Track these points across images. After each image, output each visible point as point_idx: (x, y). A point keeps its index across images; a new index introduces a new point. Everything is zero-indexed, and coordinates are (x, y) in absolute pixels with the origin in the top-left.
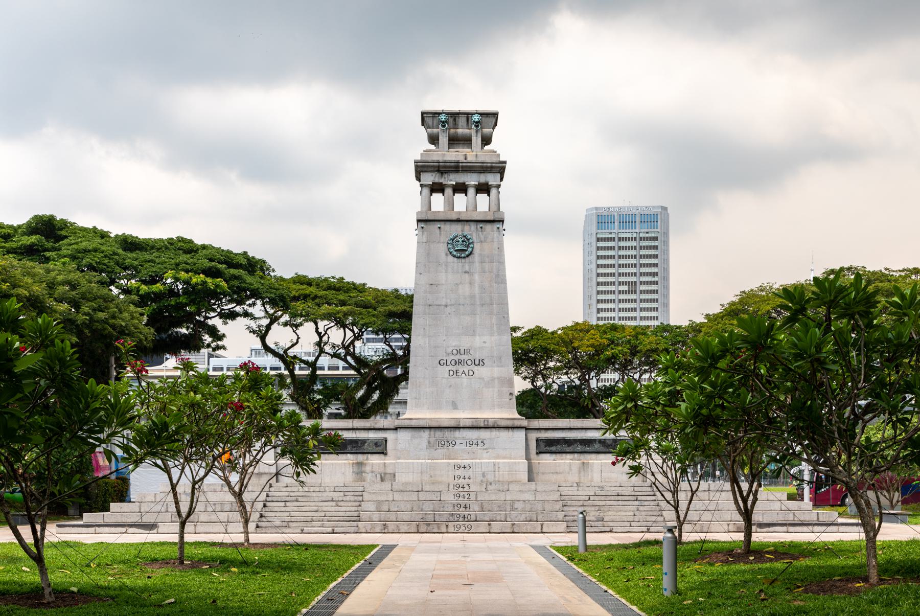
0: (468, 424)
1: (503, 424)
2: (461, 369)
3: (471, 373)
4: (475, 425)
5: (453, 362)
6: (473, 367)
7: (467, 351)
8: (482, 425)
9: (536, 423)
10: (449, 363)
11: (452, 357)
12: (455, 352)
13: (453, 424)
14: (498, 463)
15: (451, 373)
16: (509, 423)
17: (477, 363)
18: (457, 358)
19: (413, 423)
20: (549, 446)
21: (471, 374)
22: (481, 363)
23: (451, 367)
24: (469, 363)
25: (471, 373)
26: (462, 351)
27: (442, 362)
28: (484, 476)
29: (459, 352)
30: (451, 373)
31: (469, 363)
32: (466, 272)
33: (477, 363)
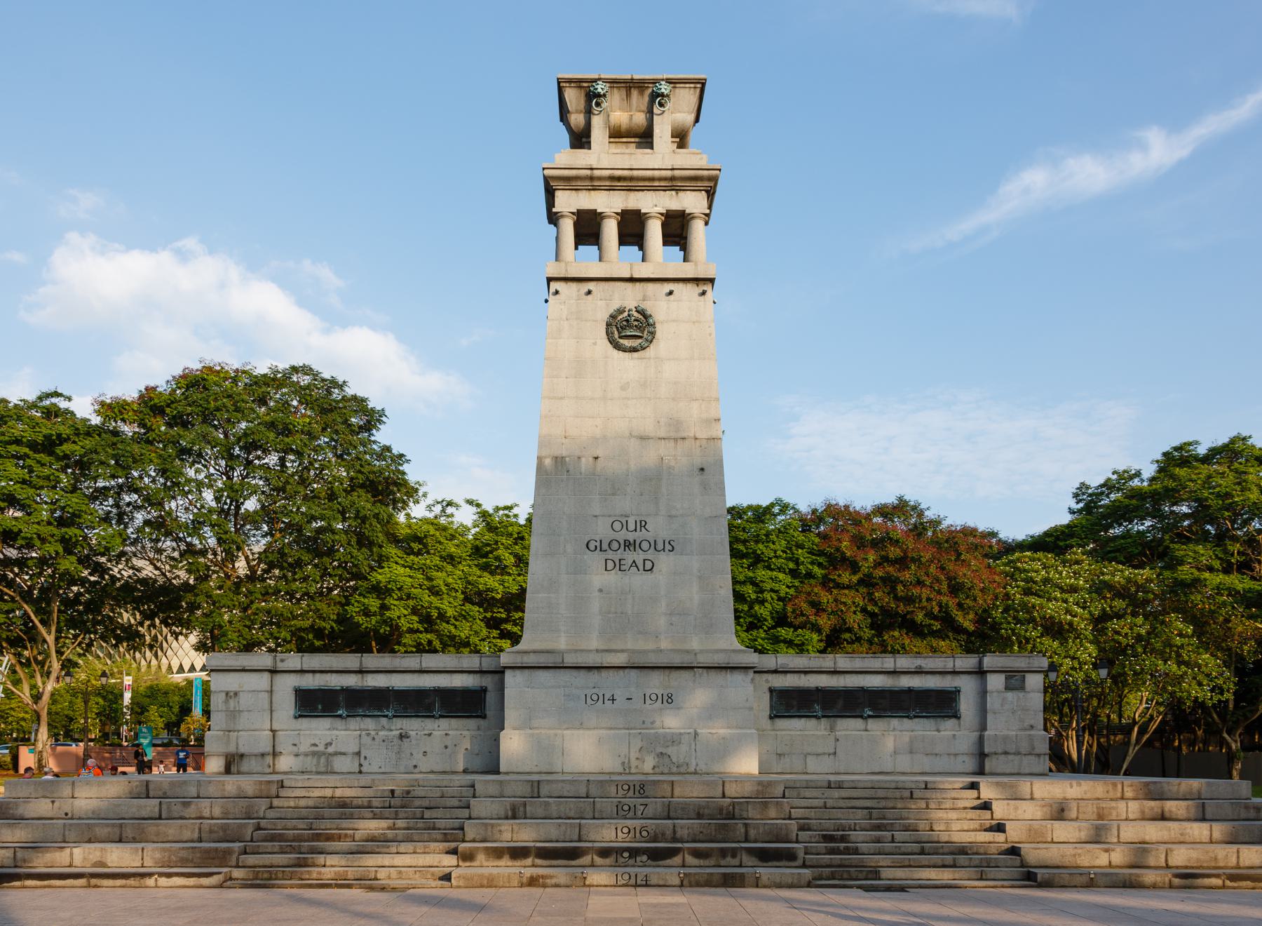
2: (630, 556)
6: (651, 555)
9: (769, 661)
10: (605, 546)
15: (610, 565)
16: (719, 659)
18: (623, 535)
20: (789, 703)
23: (610, 555)
26: (632, 527)
27: (592, 547)
30: (610, 565)
31: (645, 545)
33: (660, 547)
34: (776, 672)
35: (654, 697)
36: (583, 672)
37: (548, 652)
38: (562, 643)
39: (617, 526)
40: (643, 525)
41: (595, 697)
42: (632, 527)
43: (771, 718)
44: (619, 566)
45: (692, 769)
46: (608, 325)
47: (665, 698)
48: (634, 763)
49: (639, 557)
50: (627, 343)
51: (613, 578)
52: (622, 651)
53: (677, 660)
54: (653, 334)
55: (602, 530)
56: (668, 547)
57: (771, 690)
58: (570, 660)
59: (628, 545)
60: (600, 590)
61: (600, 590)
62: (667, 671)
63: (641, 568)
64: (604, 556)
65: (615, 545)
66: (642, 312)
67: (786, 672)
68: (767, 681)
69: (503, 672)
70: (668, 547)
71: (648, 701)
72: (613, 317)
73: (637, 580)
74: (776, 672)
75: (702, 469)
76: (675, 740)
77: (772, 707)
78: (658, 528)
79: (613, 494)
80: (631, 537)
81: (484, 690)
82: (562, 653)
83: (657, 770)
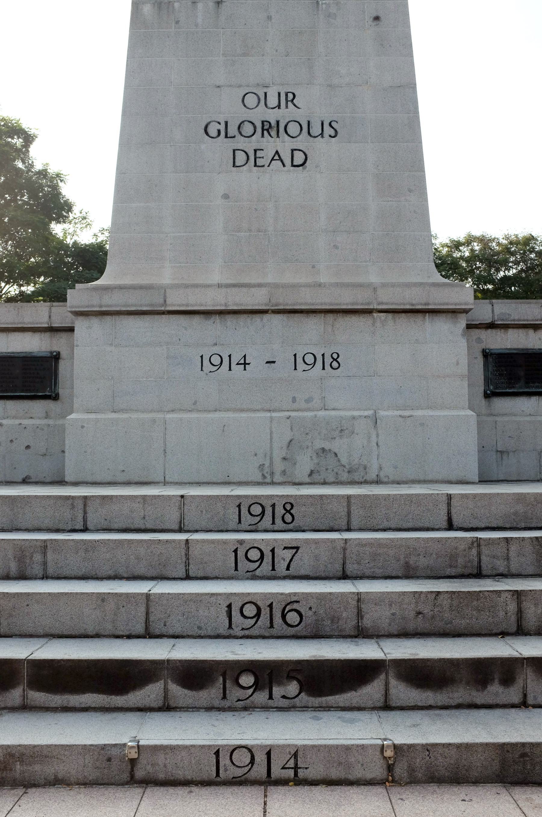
2: (270, 145)
10: (233, 130)
15: (241, 158)
16: (415, 298)
18: (259, 114)
23: (241, 143)
25: (299, 158)
26: (273, 101)
27: (213, 131)
30: (241, 158)
31: (293, 129)
33: (316, 130)
34: (492, 326)
35: (310, 359)
36: (196, 320)
37: (141, 287)
38: (166, 277)
39: (251, 100)
40: (291, 98)
41: (216, 360)
42: (273, 101)
43: (487, 396)
44: (254, 158)
45: (372, 476)
47: (328, 360)
48: (279, 466)
49: (284, 145)
51: (247, 176)
52: (260, 285)
53: (346, 300)
55: (227, 108)
56: (328, 131)
57: (486, 354)
58: (176, 301)
59: (267, 128)
60: (226, 197)
61: (226, 197)
62: (330, 317)
64: (231, 144)
65: (248, 129)
67: (506, 327)
68: (479, 340)
70: (328, 131)
71: (301, 365)
73: (282, 179)
74: (492, 326)
75: (377, 18)
76: (343, 430)
77: (487, 381)
78: (312, 105)
79: (245, 55)
80: (272, 116)
81: (56, 357)
82: (163, 289)
83: (316, 477)
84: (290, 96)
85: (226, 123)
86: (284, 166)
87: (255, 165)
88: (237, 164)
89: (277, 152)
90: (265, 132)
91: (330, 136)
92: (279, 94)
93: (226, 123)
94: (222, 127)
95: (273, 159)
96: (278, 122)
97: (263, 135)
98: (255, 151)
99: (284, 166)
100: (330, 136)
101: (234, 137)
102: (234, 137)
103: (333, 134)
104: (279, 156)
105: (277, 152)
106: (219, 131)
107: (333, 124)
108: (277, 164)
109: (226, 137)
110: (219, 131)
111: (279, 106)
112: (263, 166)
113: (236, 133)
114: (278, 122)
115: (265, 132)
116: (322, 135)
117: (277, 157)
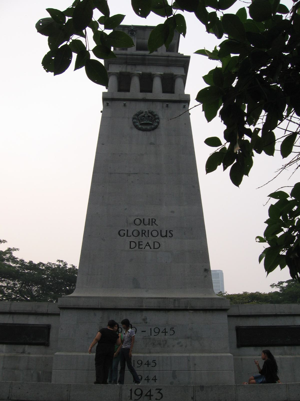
0: (153, 305)
1: (199, 305)
3: (157, 245)
4: (162, 306)
5: (135, 233)
7: (152, 222)
8: (171, 307)
10: (130, 233)
11: (134, 227)
12: (138, 222)
13: (132, 305)
14: (194, 358)
15: (133, 245)
17: (164, 234)
19: (81, 304)
21: (156, 247)
22: (169, 234)
23: (132, 239)
24: (155, 233)
25: (157, 245)
26: (147, 221)
27: (122, 233)
28: (174, 376)
29: (142, 221)
30: (133, 245)
32: (151, 144)
33: (164, 234)
46: (134, 118)
50: (144, 127)
54: (158, 123)
57: (238, 329)
59: (143, 233)
63: (152, 247)
66: (151, 113)
69: (59, 315)
70: (169, 234)
72: (137, 115)
84: (154, 220)
85: (127, 230)
86: (151, 248)
87: (139, 248)
88: (132, 247)
89: (148, 243)
90: (143, 235)
91: (169, 236)
92: (149, 219)
93: (127, 230)
94: (126, 232)
95: (146, 246)
96: (148, 231)
97: (142, 236)
98: (139, 242)
99: (151, 248)
100: (169, 236)
101: (130, 236)
102: (130, 236)
103: (171, 236)
104: (149, 244)
105: (148, 243)
106: (124, 234)
107: (171, 232)
108: (148, 248)
109: (127, 236)
110: (124, 234)
111: (149, 224)
112: (142, 248)
113: (132, 235)
114: (148, 231)
115: (143, 235)
116: (166, 236)
117: (148, 245)
